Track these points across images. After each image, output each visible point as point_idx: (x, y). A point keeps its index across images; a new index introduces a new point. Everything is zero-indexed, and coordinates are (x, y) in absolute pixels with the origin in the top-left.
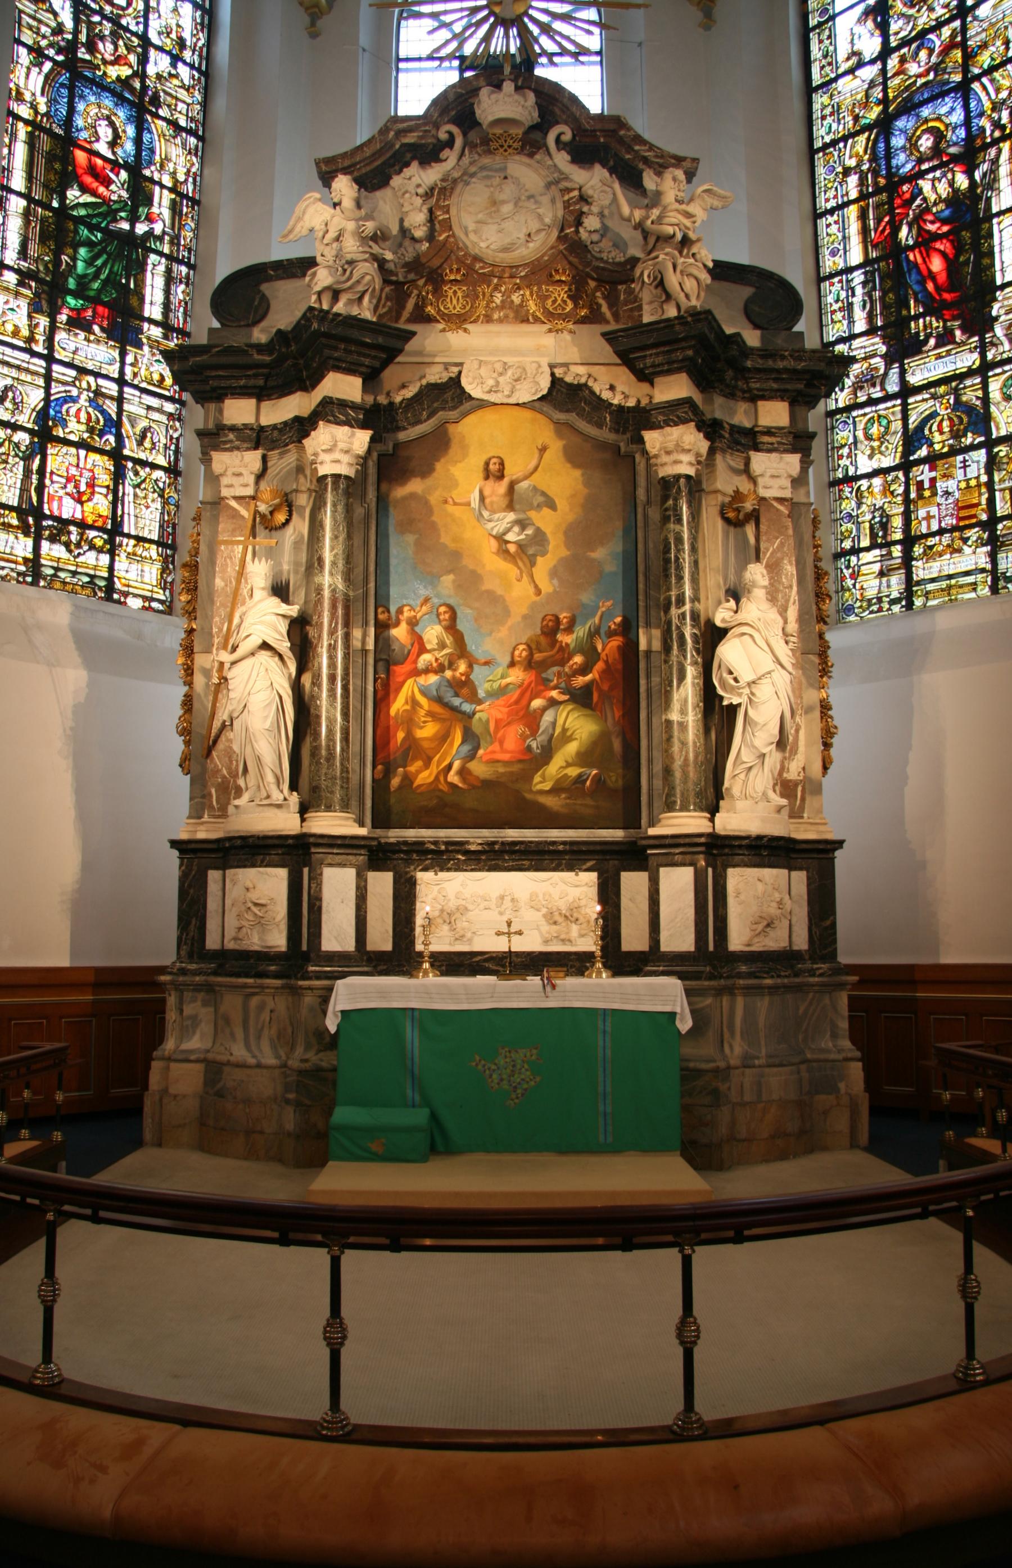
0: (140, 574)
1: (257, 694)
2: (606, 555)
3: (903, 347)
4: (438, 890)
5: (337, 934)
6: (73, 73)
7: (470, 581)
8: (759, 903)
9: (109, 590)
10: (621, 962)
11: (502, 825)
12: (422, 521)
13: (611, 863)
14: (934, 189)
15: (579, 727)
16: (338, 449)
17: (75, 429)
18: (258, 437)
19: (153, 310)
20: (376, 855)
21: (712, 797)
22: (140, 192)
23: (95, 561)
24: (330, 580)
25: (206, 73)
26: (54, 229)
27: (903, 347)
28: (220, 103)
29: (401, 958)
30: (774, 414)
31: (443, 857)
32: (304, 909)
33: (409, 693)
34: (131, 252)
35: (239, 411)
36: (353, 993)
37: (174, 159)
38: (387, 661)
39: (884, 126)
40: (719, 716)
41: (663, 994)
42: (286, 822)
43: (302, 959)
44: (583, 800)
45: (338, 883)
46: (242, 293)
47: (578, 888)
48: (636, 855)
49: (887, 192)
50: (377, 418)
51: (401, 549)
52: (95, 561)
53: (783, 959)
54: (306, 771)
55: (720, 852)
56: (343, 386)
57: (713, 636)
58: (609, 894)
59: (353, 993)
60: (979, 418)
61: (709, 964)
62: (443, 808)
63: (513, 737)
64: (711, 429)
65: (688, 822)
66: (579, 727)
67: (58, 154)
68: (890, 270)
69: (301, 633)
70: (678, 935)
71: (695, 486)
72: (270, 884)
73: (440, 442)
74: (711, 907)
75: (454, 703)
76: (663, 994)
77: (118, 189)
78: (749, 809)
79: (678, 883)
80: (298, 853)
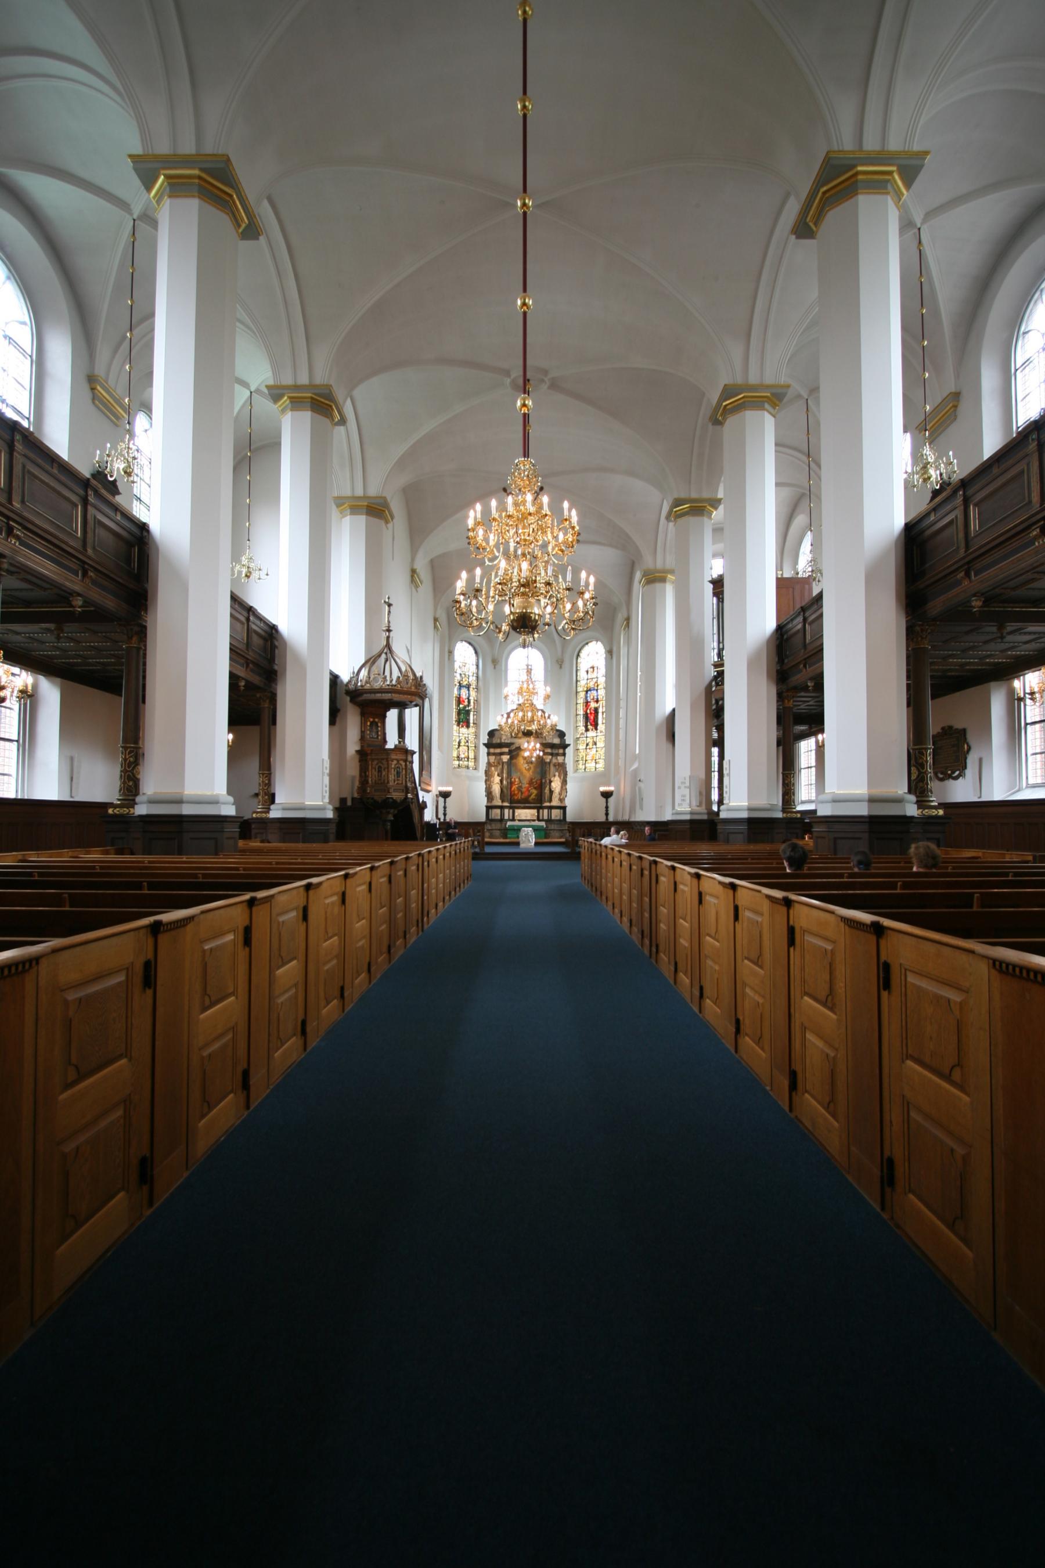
0: (471, 764)
1: (496, 789)
2: (539, 770)
3: (587, 730)
4: (518, 812)
5: (506, 817)
6: (461, 686)
7: (522, 773)
8: (556, 814)
9: (468, 767)
10: (539, 820)
11: (525, 803)
12: (515, 765)
13: (538, 809)
14: (593, 705)
15: (535, 792)
16: (505, 758)
17: (462, 744)
18: (494, 754)
19: (471, 721)
20: (509, 808)
21: (550, 801)
22: (469, 702)
23: (466, 763)
24: (505, 775)
25: (477, 677)
26: (459, 713)
27: (587, 730)
28: (480, 683)
29: (513, 820)
30: (561, 751)
31: (518, 808)
32: (502, 814)
33: (514, 787)
34: (468, 713)
35: (492, 750)
36: (509, 823)
37: (473, 694)
38: (511, 784)
39: (587, 692)
40: (551, 792)
41: (543, 824)
42: (500, 804)
43: (502, 820)
44: (535, 801)
45: (506, 811)
46: (492, 734)
47: (535, 812)
48: (543, 808)
49: (587, 703)
50: (510, 753)
51: (513, 769)
52: (466, 763)
53: (560, 820)
54: (503, 797)
55: (551, 808)
56: (506, 750)
57: (551, 782)
58: (538, 812)
59: (509, 823)
60: (595, 744)
61: (549, 821)
62: (518, 802)
63: (527, 794)
64: (552, 754)
65: (547, 804)
66: (535, 792)
67: (459, 701)
68: (586, 717)
69: (501, 781)
70: (546, 817)
71: (549, 763)
72: (498, 811)
73: (518, 755)
74: (550, 814)
75: (519, 789)
76: (543, 824)
77: (466, 703)
78: (555, 802)
79: (546, 811)
80: (502, 808)
